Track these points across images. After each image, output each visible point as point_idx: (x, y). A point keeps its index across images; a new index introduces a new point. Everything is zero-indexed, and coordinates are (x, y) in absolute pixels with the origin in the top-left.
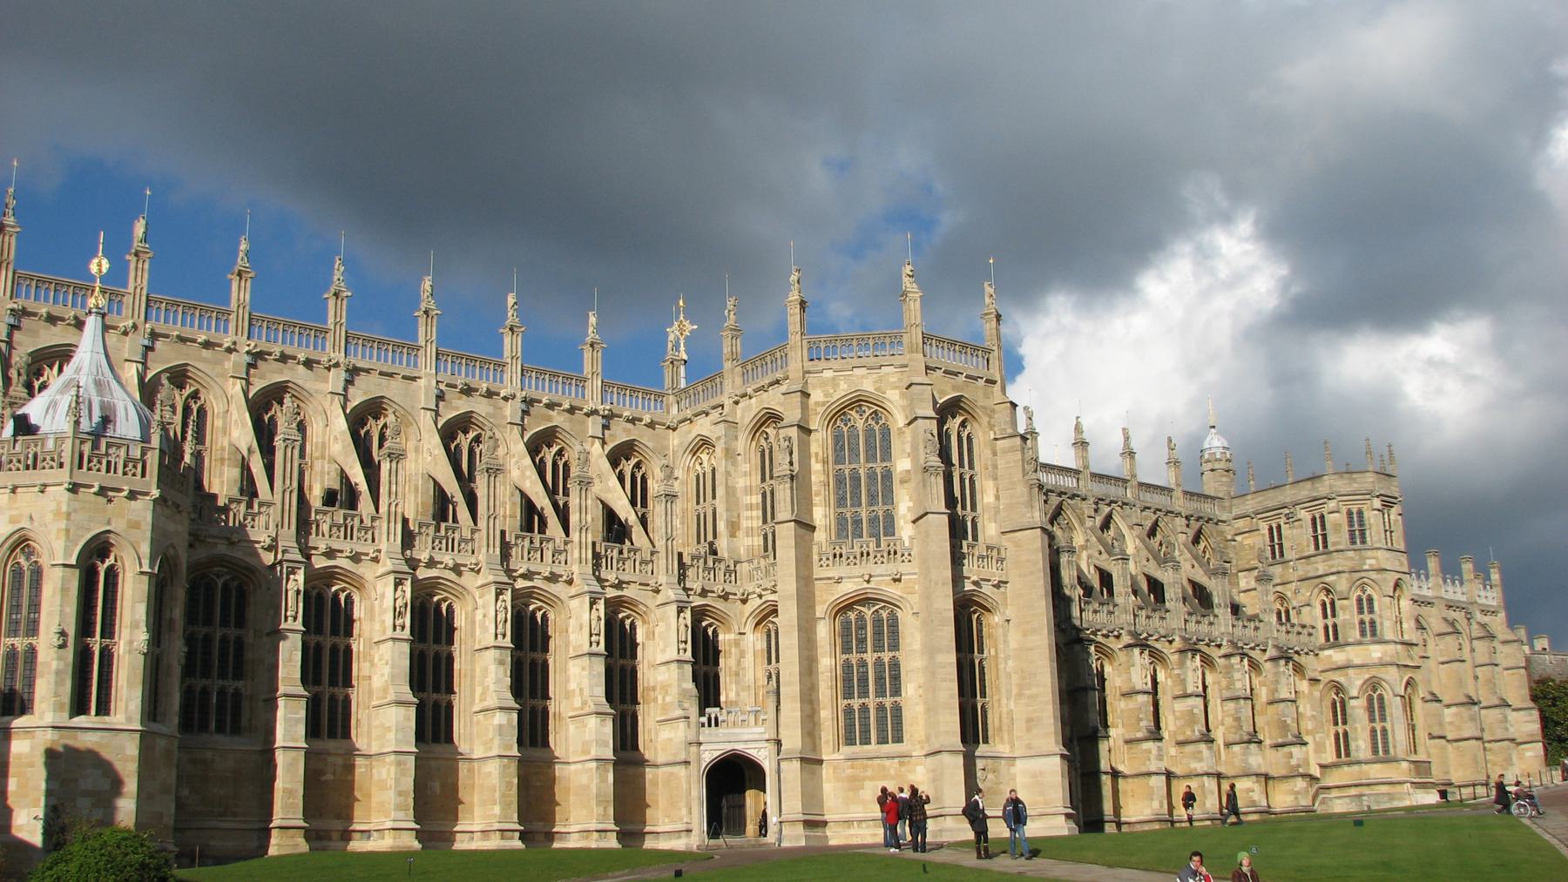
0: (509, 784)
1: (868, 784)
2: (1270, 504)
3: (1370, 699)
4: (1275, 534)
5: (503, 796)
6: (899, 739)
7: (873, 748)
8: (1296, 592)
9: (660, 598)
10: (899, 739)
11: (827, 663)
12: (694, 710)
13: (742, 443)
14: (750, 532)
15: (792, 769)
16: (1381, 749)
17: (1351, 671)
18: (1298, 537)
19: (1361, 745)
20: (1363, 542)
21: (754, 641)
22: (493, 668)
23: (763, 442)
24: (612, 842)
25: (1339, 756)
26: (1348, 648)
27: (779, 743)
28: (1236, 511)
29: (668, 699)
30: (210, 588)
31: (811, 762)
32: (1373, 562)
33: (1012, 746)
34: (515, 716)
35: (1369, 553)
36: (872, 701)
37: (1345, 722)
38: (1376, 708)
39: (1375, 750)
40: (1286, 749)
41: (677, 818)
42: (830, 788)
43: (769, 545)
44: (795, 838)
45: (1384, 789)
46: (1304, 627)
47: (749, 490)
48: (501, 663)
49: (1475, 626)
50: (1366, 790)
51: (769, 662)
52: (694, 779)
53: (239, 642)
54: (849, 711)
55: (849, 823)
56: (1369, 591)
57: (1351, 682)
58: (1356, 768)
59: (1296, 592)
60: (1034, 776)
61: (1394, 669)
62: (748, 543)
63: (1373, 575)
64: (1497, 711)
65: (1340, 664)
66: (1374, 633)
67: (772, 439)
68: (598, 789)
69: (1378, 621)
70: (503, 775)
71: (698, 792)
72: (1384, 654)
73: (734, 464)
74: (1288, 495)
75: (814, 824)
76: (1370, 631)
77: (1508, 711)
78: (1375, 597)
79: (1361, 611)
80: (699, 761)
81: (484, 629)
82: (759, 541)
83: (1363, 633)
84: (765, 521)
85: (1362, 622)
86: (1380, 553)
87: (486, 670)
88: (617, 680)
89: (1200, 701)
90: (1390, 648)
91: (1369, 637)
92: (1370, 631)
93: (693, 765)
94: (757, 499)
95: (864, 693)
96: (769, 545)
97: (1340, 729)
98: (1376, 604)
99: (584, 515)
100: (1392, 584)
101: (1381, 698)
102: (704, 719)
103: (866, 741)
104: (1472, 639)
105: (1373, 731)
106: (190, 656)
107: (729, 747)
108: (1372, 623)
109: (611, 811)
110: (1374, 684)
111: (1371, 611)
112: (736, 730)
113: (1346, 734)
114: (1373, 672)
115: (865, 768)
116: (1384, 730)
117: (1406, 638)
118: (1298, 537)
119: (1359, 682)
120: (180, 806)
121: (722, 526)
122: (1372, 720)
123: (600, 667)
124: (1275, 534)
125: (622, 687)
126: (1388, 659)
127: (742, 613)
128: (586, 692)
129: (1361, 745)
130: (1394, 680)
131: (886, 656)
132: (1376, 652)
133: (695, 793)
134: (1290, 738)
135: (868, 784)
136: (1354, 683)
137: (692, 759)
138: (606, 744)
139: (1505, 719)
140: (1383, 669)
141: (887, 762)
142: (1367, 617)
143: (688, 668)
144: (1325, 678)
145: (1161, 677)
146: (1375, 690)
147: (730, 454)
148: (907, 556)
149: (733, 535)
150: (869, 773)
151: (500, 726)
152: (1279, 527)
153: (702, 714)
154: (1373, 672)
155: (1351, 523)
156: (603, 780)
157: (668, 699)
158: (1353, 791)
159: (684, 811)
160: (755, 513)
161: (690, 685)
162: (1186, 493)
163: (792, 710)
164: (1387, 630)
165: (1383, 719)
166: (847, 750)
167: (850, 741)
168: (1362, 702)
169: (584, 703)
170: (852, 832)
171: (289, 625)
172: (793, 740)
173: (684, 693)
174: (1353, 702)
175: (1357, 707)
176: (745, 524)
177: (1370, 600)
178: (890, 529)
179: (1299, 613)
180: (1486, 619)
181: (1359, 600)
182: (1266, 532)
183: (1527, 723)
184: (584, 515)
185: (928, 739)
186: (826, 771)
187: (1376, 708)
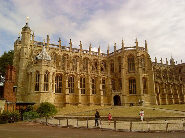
7: (133, 95)
10: (136, 93)
13: (117, 60)
21: (118, 82)
30: (58, 76)
36: (133, 89)
47: (118, 65)
53: (61, 82)
54: (130, 90)
82: (119, 71)
94: (118, 66)
99: (99, 68)
103: (132, 94)
106: (56, 84)
107: (116, 94)
120: (55, 101)
121: (114, 69)
141: (135, 96)
145: (166, 87)
148: (137, 72)
149: (116, 70)
167: (130, 94)
176: (117, 69)
178: (134, 69)
184: (99, 68)
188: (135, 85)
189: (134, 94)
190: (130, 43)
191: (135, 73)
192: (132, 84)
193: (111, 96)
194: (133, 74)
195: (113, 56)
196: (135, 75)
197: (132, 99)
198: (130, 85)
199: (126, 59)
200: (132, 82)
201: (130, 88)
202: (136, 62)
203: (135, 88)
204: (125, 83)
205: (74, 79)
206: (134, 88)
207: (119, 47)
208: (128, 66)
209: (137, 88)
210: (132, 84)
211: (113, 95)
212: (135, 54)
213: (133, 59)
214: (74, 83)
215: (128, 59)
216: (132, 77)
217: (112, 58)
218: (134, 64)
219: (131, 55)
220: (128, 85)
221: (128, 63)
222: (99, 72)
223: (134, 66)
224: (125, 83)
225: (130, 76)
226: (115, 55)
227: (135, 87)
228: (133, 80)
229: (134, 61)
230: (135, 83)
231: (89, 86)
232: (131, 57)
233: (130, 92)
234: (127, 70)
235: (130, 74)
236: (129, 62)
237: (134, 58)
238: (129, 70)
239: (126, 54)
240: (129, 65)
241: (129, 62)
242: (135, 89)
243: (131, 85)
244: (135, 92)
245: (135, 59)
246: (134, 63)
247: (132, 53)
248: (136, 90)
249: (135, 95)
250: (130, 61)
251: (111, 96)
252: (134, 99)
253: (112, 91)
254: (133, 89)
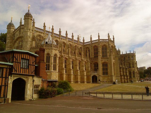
36: (105, 71)
103: (105, 75)
107: (94, 75)
131: (106, 67)
148: (109, 59)
167: (103, 74)
171: (64, 62)
190: (104, 37)
191: (107, 59)
192: (105, 67)
193: (90, 76)
194: (106, 60)
195: (90, 44)
196: (108, 61)
198: (103, 68)
199: (101, 48)
200: (105, 65)
201: (103, 70)
202: (108, 51)
203: (107, 70)
204: (100, 67)
205: (67, 61)
206: (106, 70)
207: (95, 38)
208: (102, 54)
209: (109, 70)
210: (105, 67)
211: (92, 75)
212: (107, 45)
213: (106, 49)
214: (67, 65)
215: (102, 48)
216: (105, 62)
217: (88, 46)
218: (106, 52)
219: (105, 45)
220: (102, 67)
221: (102, 51)
222: (83, 57)
224: (100, 67)
226: (91, 44)
227: (107, 69)
228: (106, 64)
229: (106, 50)
231: (77, 67)
233: (104, 73)
234: (101, 57)
237: (106, 48)
238: (102, 57)
239: (101, 44)
240: (103, 53)
241: (103, 51)
243: (104, 68)
244: (107, 73)
245: (107, 49)
247: (105, 44)
248: (107, 72)
250: (104, 50)
251: (90, 76)
253: (91, 72)
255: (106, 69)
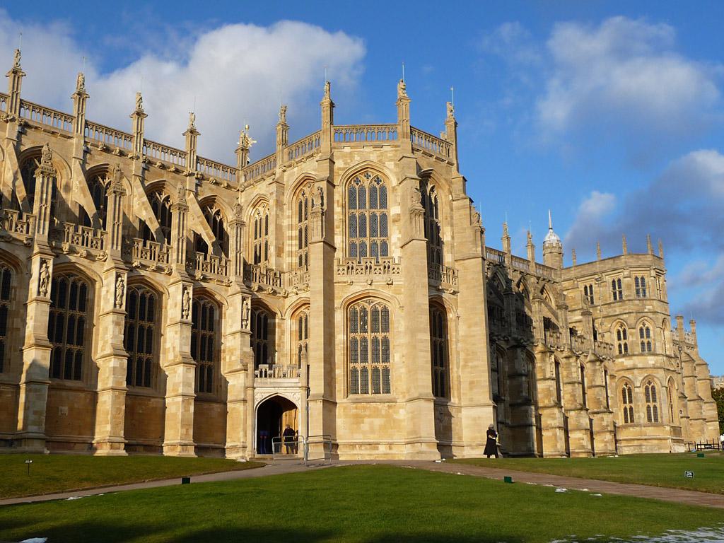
0: (119, 409)
1: (366, 420)
2: (585, 273)
3: (647, 389)
4: (588, 291)
5: (114, 417)
6: (388, 391)
8: (601, 324)
9: (231, 290)
11: (340, 338)
12: (251, 366)
14: (291, 254)
15: (317, 408)
16: (653, 416)
17: (636, 371)
18: (603, 292)
19: (641, 415)
20: (644, 295)
22: (111, 327)
23: (301, 197)
24: (191, 453)
25: (626, 421)
26: (634, 358)
27: (308, 389)
28: (564, 277)
29: (233, 358)
31: (329, 403)
32: (651, 307)
33: (460, 399)
34: (125, 362)
35: (648, 302)
37: (631, 402)
38: (651, 394)
39: (649, 419)
40: (600, 416)
41: (240, 437)
42: (341, 422)
43: (304, 261)
44: (317, 453)
45: (656, 442)
46: (607, 344)
48: (117, 324)
49: (683, 355)
50: (644, 443)
51: (301, 339)
52: (249, 412)
55: (353, 445)
56: (647, 325)
57: (636, 378)
58: (638, 429)
59: (601, 324)
60: (474, 419)
61: (661, 372)
62: (289, 261)
63: (650, 315)
64: (696, 403)
65: (629, 367)
66: (649, 349)
67: (307, 195)
68: (183, 415)
69: (652, 342)
70: (114, 403)
71: (251, 421)
72: (656, 362)
73: (282, 210)
74: (598, 268)
75: (331, 445)
76: (647, 348)
77: (702, 404)
78: (651, 328)
79: (642, 337)
80: (253, 400)
81: (107, 301)
83: (643, 349)
84: (300, 248)
85: (643, 343)
86: (655, 303)
87: (106, 328)
88: (199, 343)
89: (554, 383)
90: (660, 358)
91: (647, 351)
92: (647, 348)
93: (249, 403)
94: (295, 233)
95: (365, 360)
96: (304, 261)
97: (628, 406)
98: (651, 333)
100: (661, 321)
101: (653, 388)
102: (257, 372)
104: (681, 362)
105: (649, 407)
108: (649, 343)
109: (191, 432)
110: (648, 381)
111: (648, 336)
112: (279, 380)
113: (631, 409)
114: (650, 372)
115: (365, 409)
116: (655, 407)
117: (668, 353)
118: (603, 292)
119: (641, 378)
122: (648, 401)
123: (188, 333)
124: (588, 291)
125: (204, 349)
126: (659, 365)
127: (283, 306)
128: (178, 349)
129: (641, 415)
130: (661, 379)
132: (651, 360)
133: (249, 422)
134: (602, 409)
135: (366, 420)
136: (638, 378)
137: (249, 398)
138: (190, 386)
139: (701, 407)
140: (655, 371)
141: (380, 406)
142: (645, 340)
143: (248, 338)
144: (618, 375)
146: (650, 383)
147: (279, 204)
150: (367, 413)
151: (114, 368)
152: (591, 286)
153: (256, 368)
154: (650, 372)
155: (637, 285)
156: (186, 410)
157: (233, 358)
158: (636, 443)
159: (241, 434)
160: (294, 242)
161: (249, 349)
162: (537, 264)
163: (318, 370)
164: (659, 351)
165: (654, 400)
166: (351, 396)
168: (642, 390)
169: (175, 357)
170: (355, 452)
172: (318, 387)
173: (244, 354)
174: (637, 390)
175: (639, 392)
176: (287, 249)
177: (648, 329)
179: (603, 336)
180: (688, 351)
181: (641, 330)
182: (583, 289)
183: (711, 411)
185: (408, 392)
186: (339, 411)
187: (651, 394)
188: (386, 341)
189: (377, 392)
197: (365, 426)
203: (386, 359)
206: (376, 359)
210: (369, 336)
216: (365, 297)
223: (384, 232)
225: (357, 289)
228: (375, 312)
230: (386, 329)
232: (367, 184)
235: (363, 277)
236: (357, 213)
237: (383, 190)
242: (381, 366)
243: (365, 340)
245: (390, 197)
246: (384, 217)
248: (387, 371)
249: (382, 396)
252: (378, 422)
254: (369, 366)
255: (375, 350)
